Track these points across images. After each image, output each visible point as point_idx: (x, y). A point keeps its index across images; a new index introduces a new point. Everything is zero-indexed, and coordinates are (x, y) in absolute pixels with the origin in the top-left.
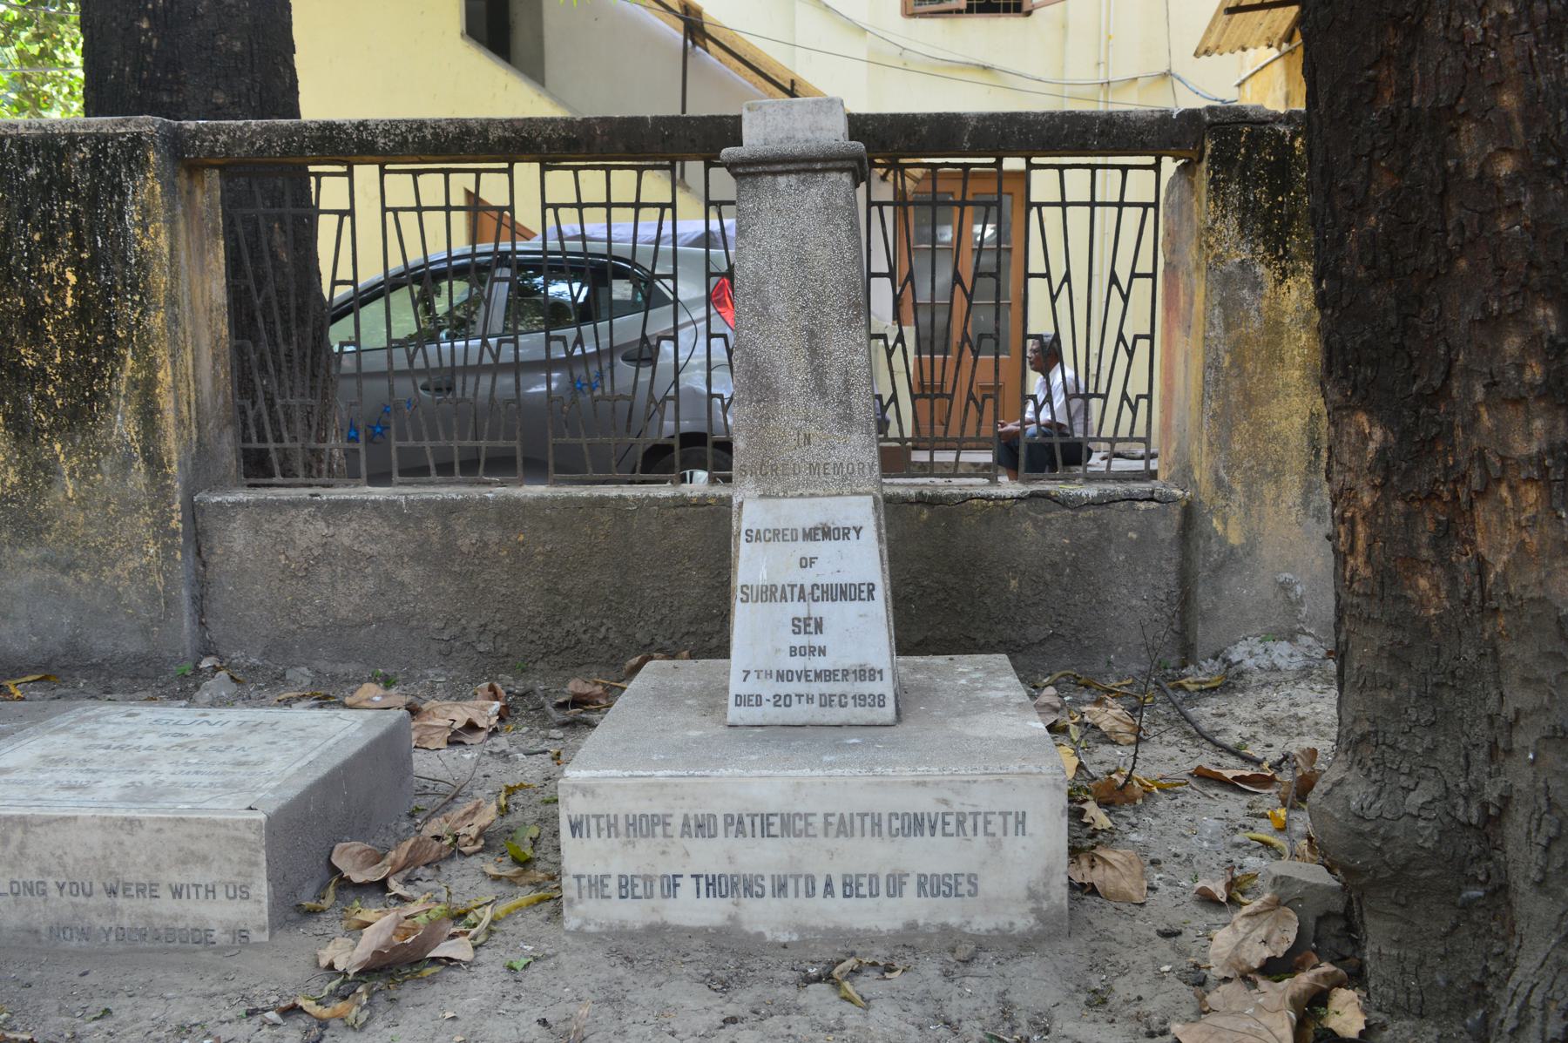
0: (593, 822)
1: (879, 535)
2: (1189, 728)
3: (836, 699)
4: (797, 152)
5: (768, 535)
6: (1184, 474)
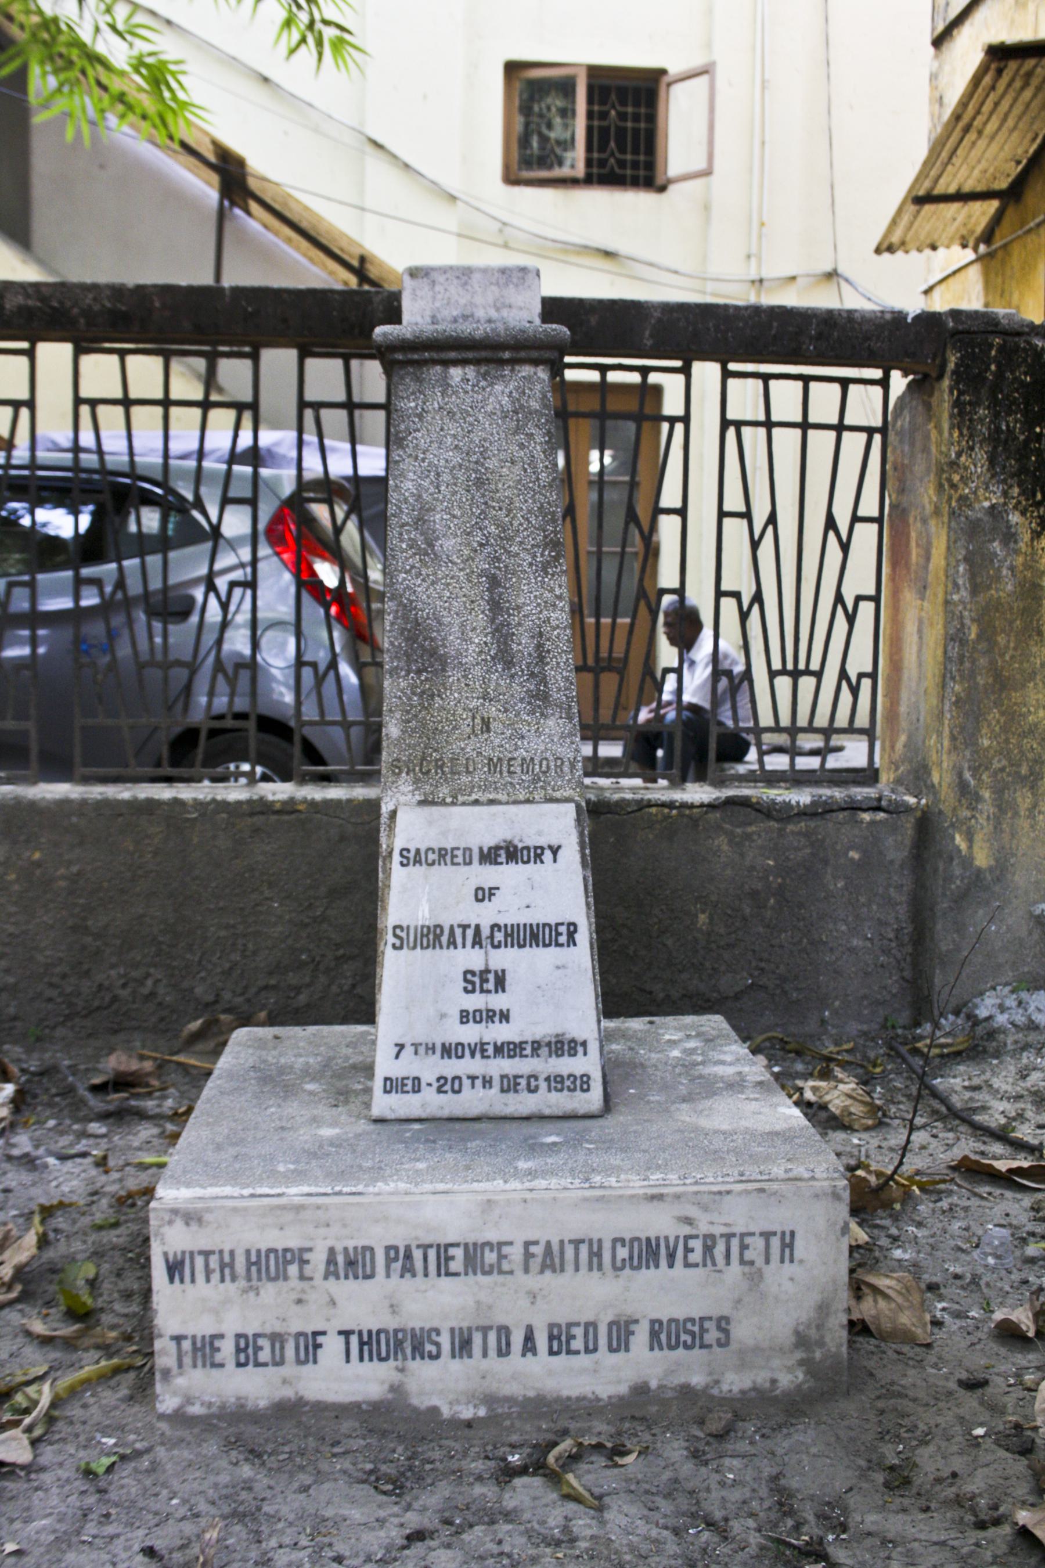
0: (199, 1261)
2: (936, 1104)
3: (523, 1082)
4: (479, 334)
5: (431, 857)
6: (918, 776)
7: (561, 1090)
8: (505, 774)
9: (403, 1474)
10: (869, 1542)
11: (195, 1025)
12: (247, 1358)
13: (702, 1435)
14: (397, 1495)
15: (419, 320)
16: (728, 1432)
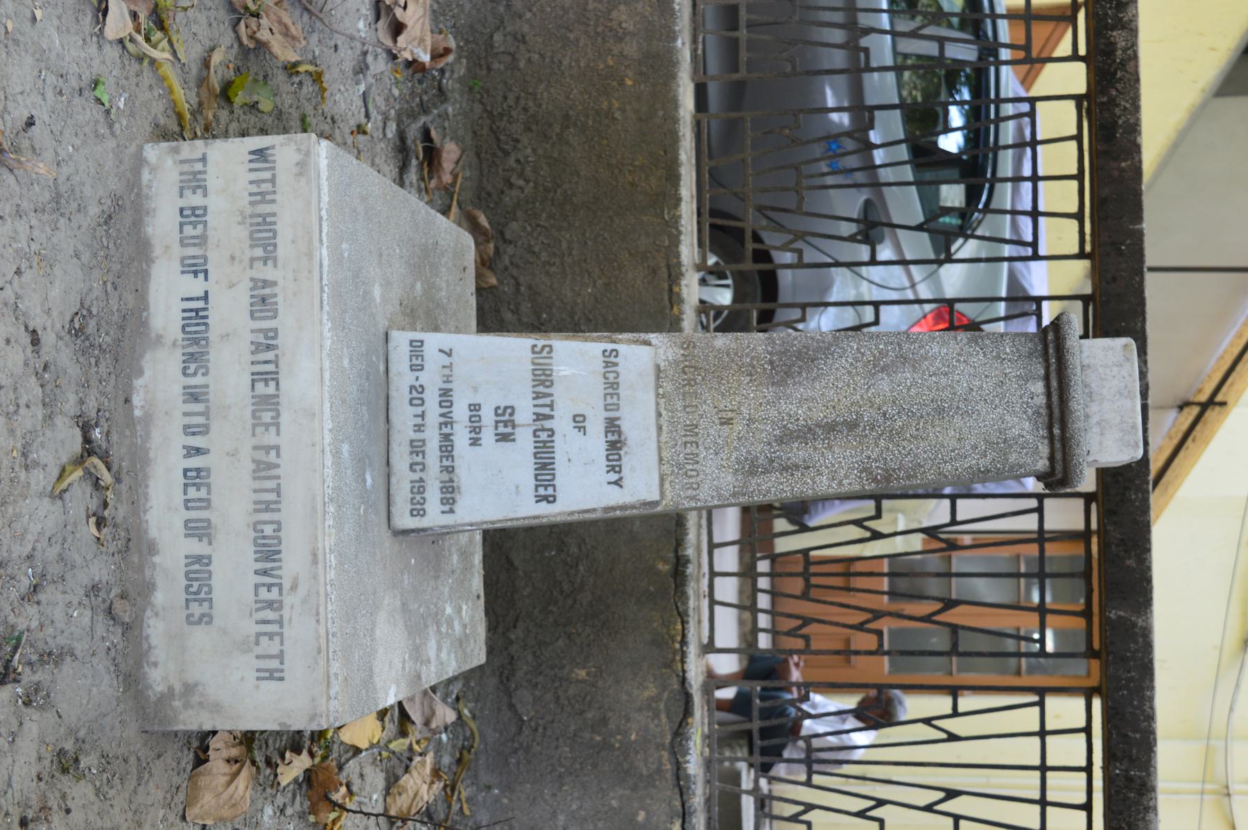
0: (266, 175)
1: (613, 509)
3: (419, 459)
4: (1073, 405)
5: (611, 376)
7: (412, 492)
8: (684, 439)
9: (87, 338)
11: (483, 220)
12: (187, 216)
13: (112, 596)
14: (69, 332)
15: (1085, 355)
16: (113, 619)
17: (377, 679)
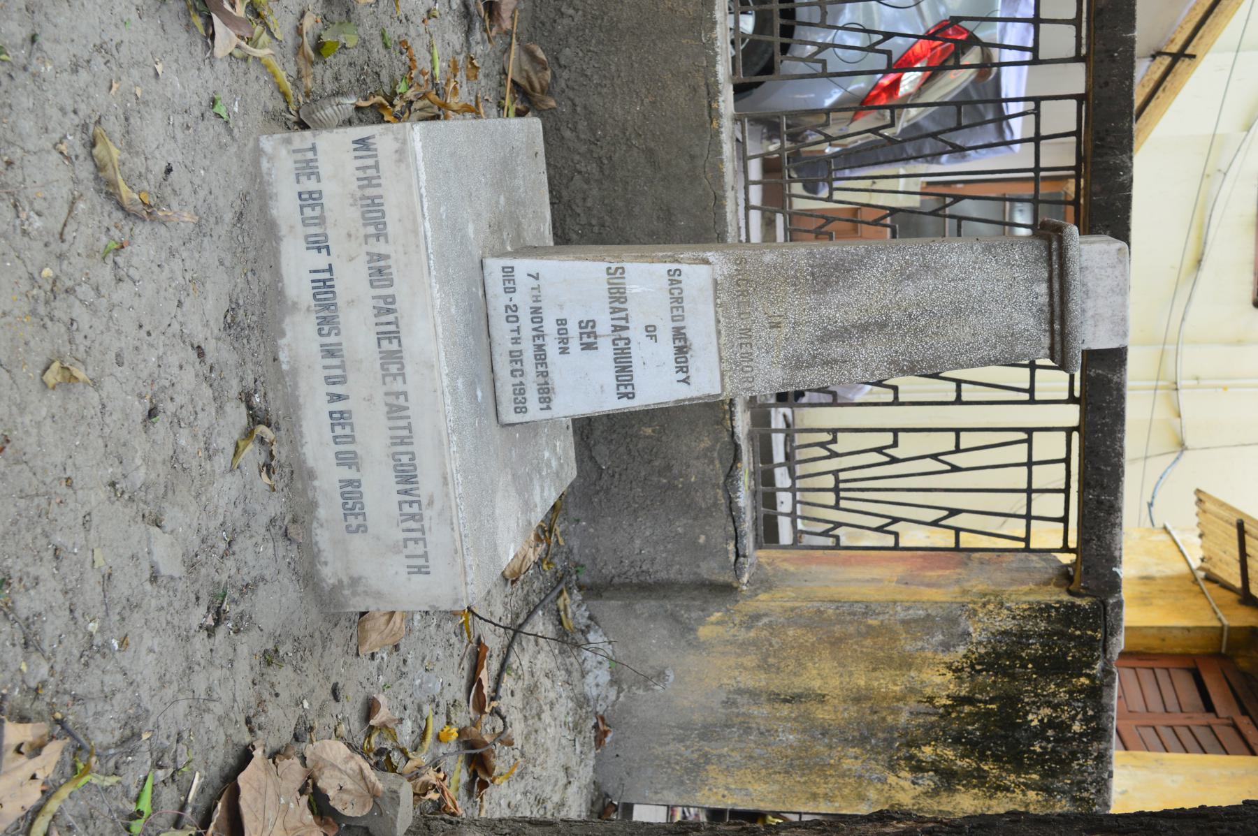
0: (371, 162)
1: (684, 400)
2: (523, 616)
3: (518, 366)
4: (1072, 306)
5: (676, 292)
6: (764, 583)
10: (230, 650)
11: (540, 54)
15: (1083, 258)
17: (500, 549)
